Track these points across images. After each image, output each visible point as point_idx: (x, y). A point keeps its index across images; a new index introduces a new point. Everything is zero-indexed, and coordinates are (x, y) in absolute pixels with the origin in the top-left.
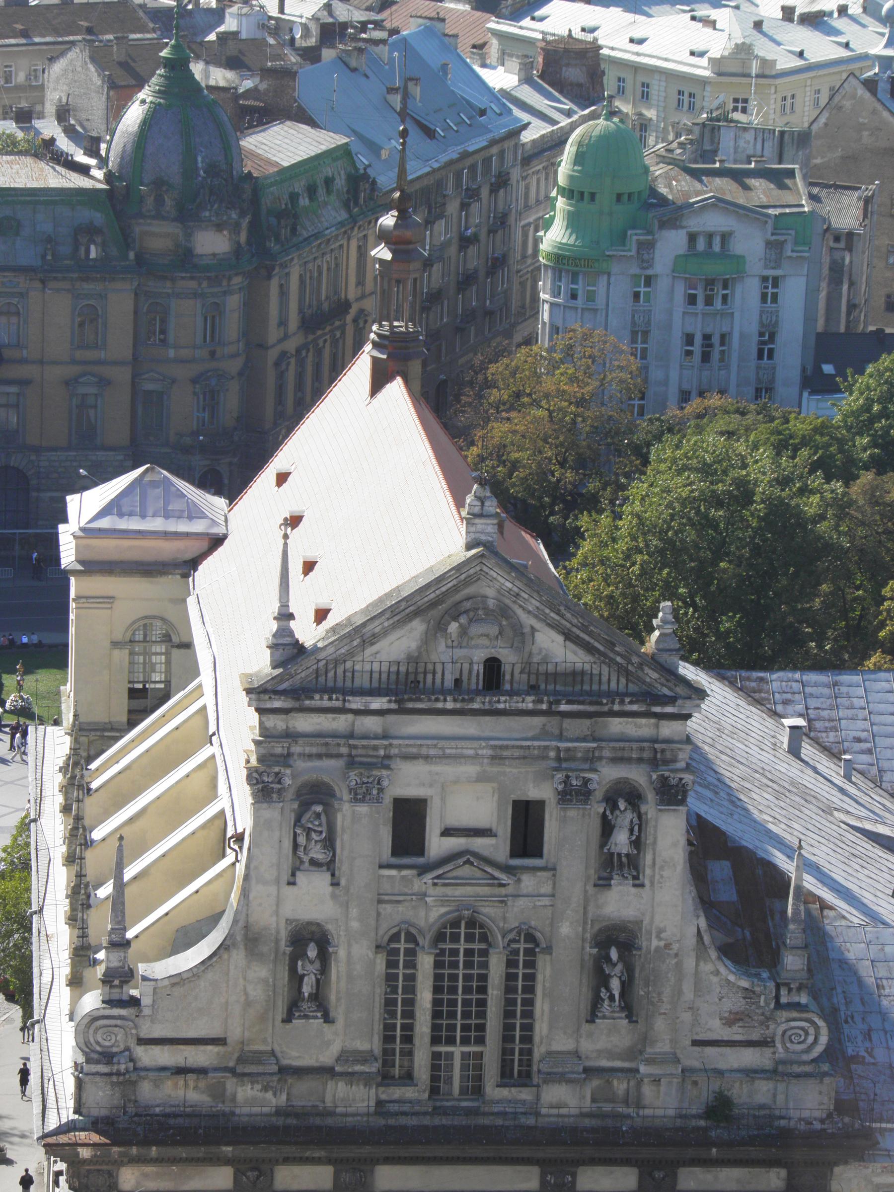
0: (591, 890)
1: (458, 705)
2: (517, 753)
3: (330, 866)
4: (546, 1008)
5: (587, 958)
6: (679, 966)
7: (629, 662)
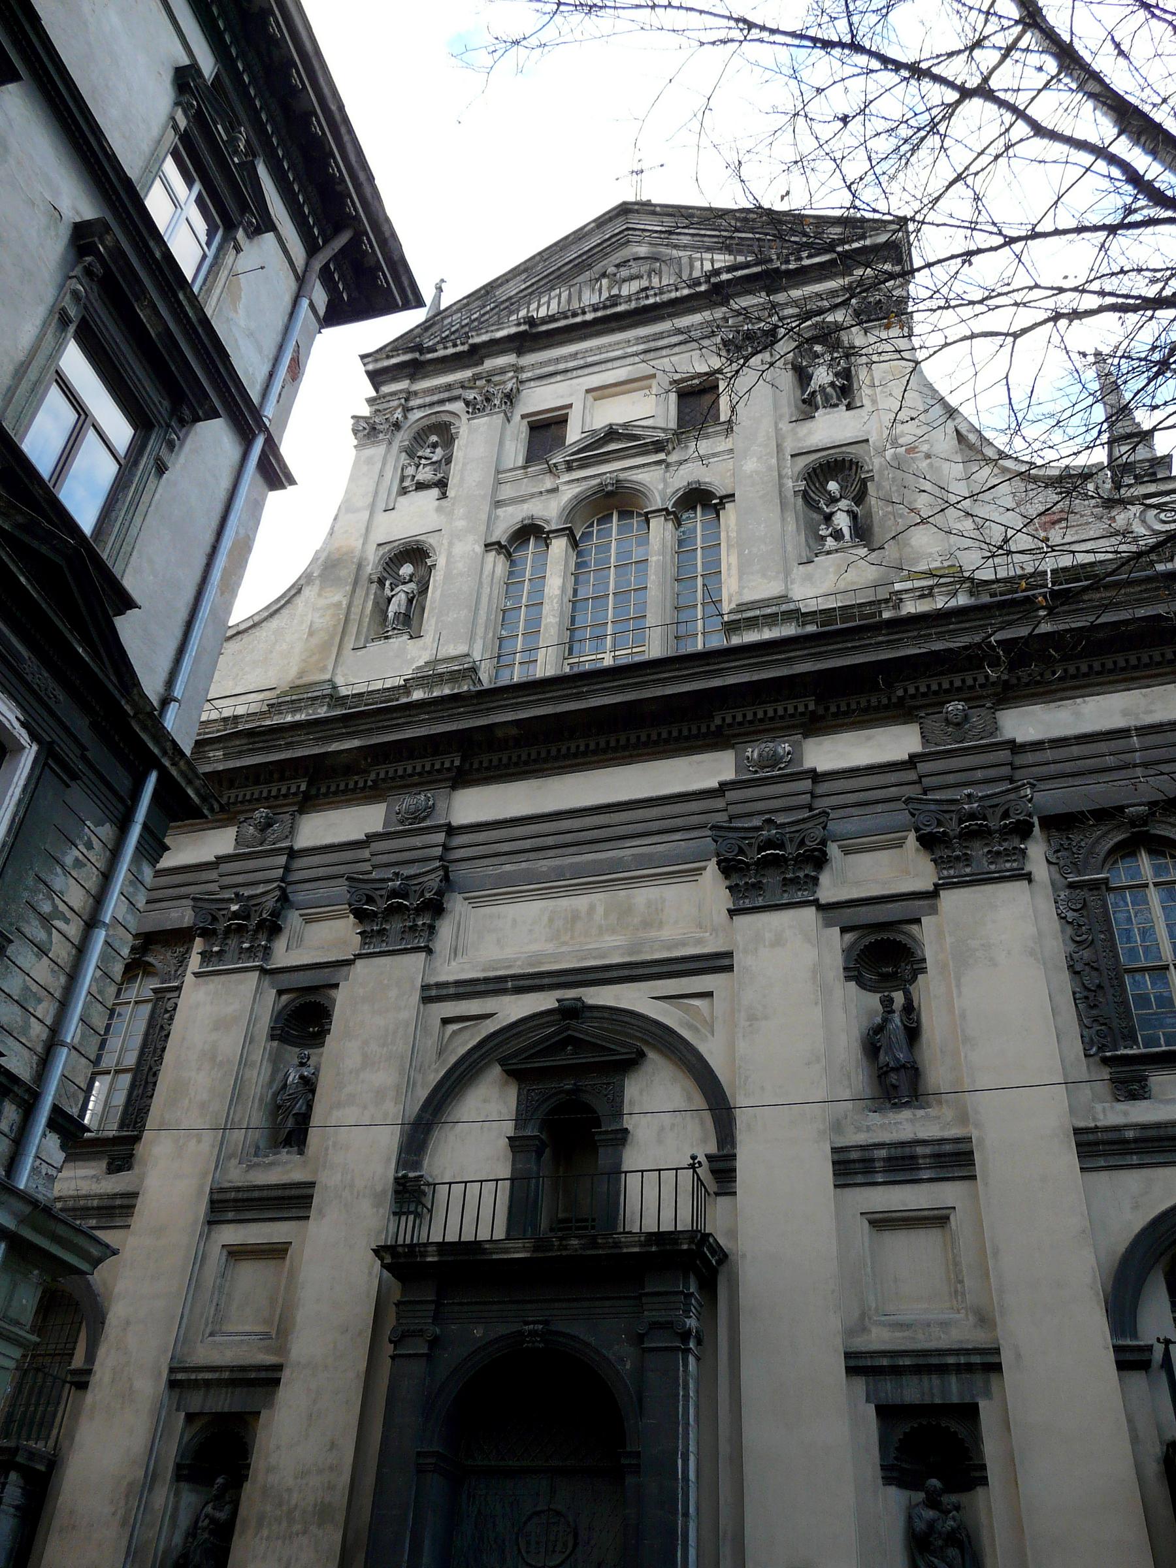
0: (785, 426)
1: (599, 314)
3: (442, 484)
4: (734, 560)
7: (805, 234)
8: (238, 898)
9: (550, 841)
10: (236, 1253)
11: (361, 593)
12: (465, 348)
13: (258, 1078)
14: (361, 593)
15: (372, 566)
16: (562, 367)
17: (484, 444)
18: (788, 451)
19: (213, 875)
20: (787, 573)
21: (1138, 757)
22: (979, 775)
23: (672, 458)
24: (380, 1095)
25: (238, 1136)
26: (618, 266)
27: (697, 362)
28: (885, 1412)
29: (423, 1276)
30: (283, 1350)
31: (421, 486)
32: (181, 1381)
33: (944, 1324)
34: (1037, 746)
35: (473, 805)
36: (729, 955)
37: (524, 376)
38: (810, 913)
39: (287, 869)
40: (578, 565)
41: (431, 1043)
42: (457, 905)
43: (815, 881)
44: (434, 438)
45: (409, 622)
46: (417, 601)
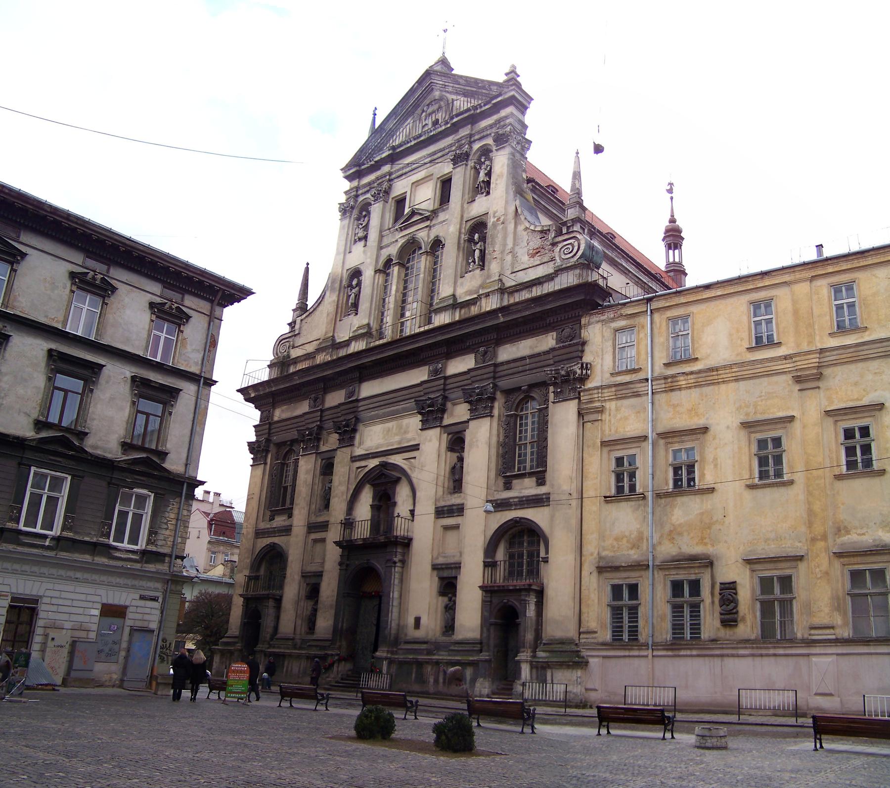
0: (466, 206)
2: (439, 154)
3: (365, 238)
5: (462, 242)
6: (505, 230)
8: (308, 429)
9: (382, 403)
10: (315, 541)
11: (342, 294)
12: (373, 163)
13: (318, 488)
14: (342, 294)
15: (344, 283)
16: (404, 171)
17: (379, 214)
18: (465, 219)
19: (303, 419)
20: (455, 283)
21: (527, 367)
22: (485, 376)
23: (434, 222)
24: (343, 493)
25: (313, 507)
26: (428, 105)
27: (445, 168)
28: (441, 579)
29: (348, 547)
30: (323, 567)
31: (360, 239)
32: (305, 575)
33: (454, 556)
34: (502, 364)
35: (369, 389)
36: (419, 445)
37: (394, 176)
38: (438, 429)
39: (321, 416)
40: (406, 275)
41: (353, 476)
42: (361, 427)
43: (442, 418)
44: (364, 213)
45: (356, 306)
46: (357, 296)
